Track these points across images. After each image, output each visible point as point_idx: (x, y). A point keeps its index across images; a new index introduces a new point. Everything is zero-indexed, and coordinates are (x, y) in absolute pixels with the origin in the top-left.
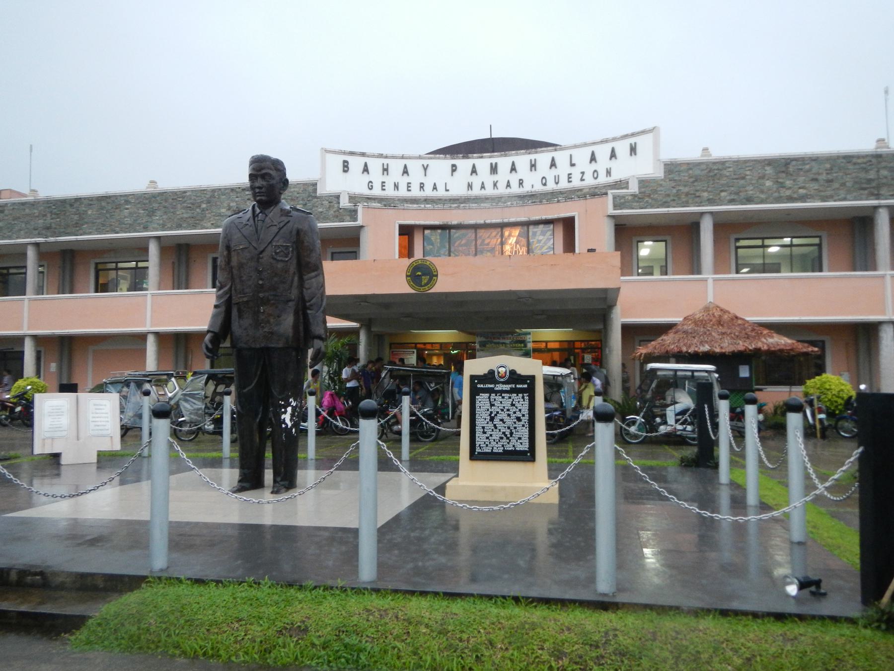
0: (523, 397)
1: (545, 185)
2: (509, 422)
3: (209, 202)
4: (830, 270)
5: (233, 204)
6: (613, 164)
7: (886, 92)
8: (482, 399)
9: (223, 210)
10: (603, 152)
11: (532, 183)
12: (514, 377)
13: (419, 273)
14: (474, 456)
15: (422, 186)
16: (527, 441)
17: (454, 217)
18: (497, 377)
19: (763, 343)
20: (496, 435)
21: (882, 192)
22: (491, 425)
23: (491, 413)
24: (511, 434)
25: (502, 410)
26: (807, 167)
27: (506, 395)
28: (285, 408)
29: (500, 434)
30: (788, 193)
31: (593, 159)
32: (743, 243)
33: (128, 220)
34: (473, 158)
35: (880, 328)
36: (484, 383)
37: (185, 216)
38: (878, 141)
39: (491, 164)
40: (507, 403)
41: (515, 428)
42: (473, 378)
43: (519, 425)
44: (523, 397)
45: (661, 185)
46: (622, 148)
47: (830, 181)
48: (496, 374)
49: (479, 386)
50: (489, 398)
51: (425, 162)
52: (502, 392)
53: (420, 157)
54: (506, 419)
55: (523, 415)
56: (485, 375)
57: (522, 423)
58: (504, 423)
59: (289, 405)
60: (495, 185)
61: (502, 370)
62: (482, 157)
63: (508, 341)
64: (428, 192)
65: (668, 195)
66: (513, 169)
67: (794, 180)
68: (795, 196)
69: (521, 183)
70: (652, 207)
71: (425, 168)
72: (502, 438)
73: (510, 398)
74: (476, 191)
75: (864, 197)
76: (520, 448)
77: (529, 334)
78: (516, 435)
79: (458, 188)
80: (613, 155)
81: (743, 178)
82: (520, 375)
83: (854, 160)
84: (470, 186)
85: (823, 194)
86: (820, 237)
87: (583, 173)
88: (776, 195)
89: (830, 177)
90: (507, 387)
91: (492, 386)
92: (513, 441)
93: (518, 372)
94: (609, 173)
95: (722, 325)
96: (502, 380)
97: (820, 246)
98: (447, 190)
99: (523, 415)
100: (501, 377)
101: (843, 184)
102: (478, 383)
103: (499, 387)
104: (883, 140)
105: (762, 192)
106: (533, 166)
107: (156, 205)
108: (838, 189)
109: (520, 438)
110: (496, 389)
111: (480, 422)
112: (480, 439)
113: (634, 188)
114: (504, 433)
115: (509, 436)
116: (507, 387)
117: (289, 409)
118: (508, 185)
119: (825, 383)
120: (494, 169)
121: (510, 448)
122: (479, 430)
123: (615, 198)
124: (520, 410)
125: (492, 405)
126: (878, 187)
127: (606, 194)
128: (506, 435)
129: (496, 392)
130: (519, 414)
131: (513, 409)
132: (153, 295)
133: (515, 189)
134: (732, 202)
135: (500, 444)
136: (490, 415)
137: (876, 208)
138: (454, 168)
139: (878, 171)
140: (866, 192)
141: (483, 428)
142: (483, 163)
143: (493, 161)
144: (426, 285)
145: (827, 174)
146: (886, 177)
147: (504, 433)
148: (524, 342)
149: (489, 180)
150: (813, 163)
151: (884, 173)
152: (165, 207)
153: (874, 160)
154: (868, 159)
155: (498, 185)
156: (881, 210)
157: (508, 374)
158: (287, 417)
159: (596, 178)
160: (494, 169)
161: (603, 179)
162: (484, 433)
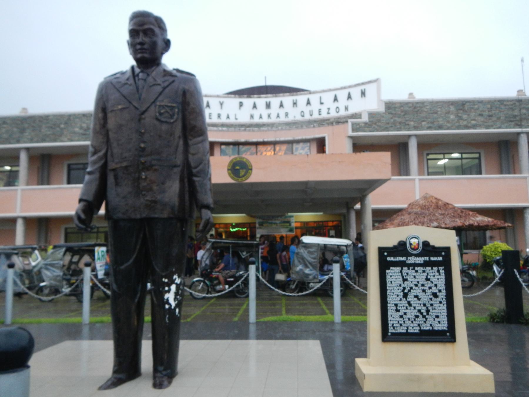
0: (438, 271)
1: (303, 116)
3: (66, 123)
4: (487, 174)
5: (84, 125)
6: (350, 103)
7: (522, 60)
8: (393, 273)
9: (77, 130)
10: (342, 95)
11: (295, 115)
12: (428, 249)
13: (238, 168)
14: (387, 336)
15: (219, 116)
16: (446, 319)
17: (242, 137)
18: (409, 249)
19: (473, 220)
20: (411, 313)
21: (523, 124)
22: (404, 302)
23: (404, 288)
24: (428, 311)
25: (416, 285)
26: (476, 106)
27: (420, 269)
28: (169, 285)
29: (415, 312)
30: (465, 123)
31: (336, 99)
32: (431, 156)
33: (5, 136)
34: (254, 98)
35: (525, 211)
36: (395, 256)
37: (49, 133)
38: (519, 91)
39: (267, 103)
40: (421, 278)
41: (432, 305)
42: (381, 250)
43: (435, 301)
44: (438, 271)
45: (383, 117)
46: (356, 92)
47: (490, 116)
48: (408, 245)
49: (389, 259)
50: (401, 272)
51: (221, 100)
52: (415, 265)
53: (218, 96)
54: (421, 295)
55: (440, 291)
56: (395, 247)
57: (439, 299)
58: (419, 299)
59: (172, 282)
60: (269, 116)
61: (414, 241)
62: (260, 97)
63: (278, 222)
64: (224, 120)
65: (388, 123)
66: (281, 105)
67: (468, 115)
68: (469, 125)
69: (287, 115)
70: (378, 131)
71: (221, 104)
72: (417, 317)
73: (424, 272)
74: (256, 120)
75: (512, 126)
76: (438, 327)
77: (292, 216)
78: (433, 313)
79: (244, 117)
80: (349, 97)
81: (436, 113)
82: (433, 247)
83: (505, 103)
84: (252, 117)
85: (486, 124)
86: (480, 153)
87: (329, 109)
88: (457, 124)
89: (490, 113)
91: (403, 259)
92: (430, 319)
93: (432, 243)
94: (346, 108)
95: (440, 209)
96: (415, 252)
97: (479, 158)
98: (236, 119)
99: (440, 291)
100: (414, 249)
101: (499, 118)
102: (387, 256)
103: (412, 260)
104: (522, 91)
105: (448, 122)
106: (295, 104)
107: (26, 125)
108: (496, 121)
109: (437, 317)
110: (408, 262)
111: (392, 299)
112: (393, 317)
113: (365, 118)
115: (425, 314)
116: (420, 260)
117: (173, 287)
118: (278, 116)
119: (498, 248)
120: (268, 106)
121: (426, 327)
123: (353, 124)
124: (436, 285)
125: (405, 280)
126: (521, 120)
127: (347, 122)
128: (422, 314)
129: (409, 266)
130: (434, 290)
131: (428, 284)
132: (23, 190)
133: (283, 119)
134: (429, 128)
135: (415, 323)
136: (403, 291)
137: (518, 134)
138: (241, 104)
139: (520, 110)
140: (513, 123)
141: (396, 305)
142: (261, 101)
143: (268, 100)
144: (243, 176)
145: (489, 111)
146: (525, 114)
147: (419, 311)
148: (289, 222)
149: (265, 113)
150: (480, 105)
151: (524, 111)
152: (33, 126)
153: (517, 104)
154: (514, 102)
155: (271, 116)
156: (522, 135)
157: (421, 245)
158: (170, 297)
159: (338, 112)
160: (268, 106)
161: (343, 113)
162: (397, 311)
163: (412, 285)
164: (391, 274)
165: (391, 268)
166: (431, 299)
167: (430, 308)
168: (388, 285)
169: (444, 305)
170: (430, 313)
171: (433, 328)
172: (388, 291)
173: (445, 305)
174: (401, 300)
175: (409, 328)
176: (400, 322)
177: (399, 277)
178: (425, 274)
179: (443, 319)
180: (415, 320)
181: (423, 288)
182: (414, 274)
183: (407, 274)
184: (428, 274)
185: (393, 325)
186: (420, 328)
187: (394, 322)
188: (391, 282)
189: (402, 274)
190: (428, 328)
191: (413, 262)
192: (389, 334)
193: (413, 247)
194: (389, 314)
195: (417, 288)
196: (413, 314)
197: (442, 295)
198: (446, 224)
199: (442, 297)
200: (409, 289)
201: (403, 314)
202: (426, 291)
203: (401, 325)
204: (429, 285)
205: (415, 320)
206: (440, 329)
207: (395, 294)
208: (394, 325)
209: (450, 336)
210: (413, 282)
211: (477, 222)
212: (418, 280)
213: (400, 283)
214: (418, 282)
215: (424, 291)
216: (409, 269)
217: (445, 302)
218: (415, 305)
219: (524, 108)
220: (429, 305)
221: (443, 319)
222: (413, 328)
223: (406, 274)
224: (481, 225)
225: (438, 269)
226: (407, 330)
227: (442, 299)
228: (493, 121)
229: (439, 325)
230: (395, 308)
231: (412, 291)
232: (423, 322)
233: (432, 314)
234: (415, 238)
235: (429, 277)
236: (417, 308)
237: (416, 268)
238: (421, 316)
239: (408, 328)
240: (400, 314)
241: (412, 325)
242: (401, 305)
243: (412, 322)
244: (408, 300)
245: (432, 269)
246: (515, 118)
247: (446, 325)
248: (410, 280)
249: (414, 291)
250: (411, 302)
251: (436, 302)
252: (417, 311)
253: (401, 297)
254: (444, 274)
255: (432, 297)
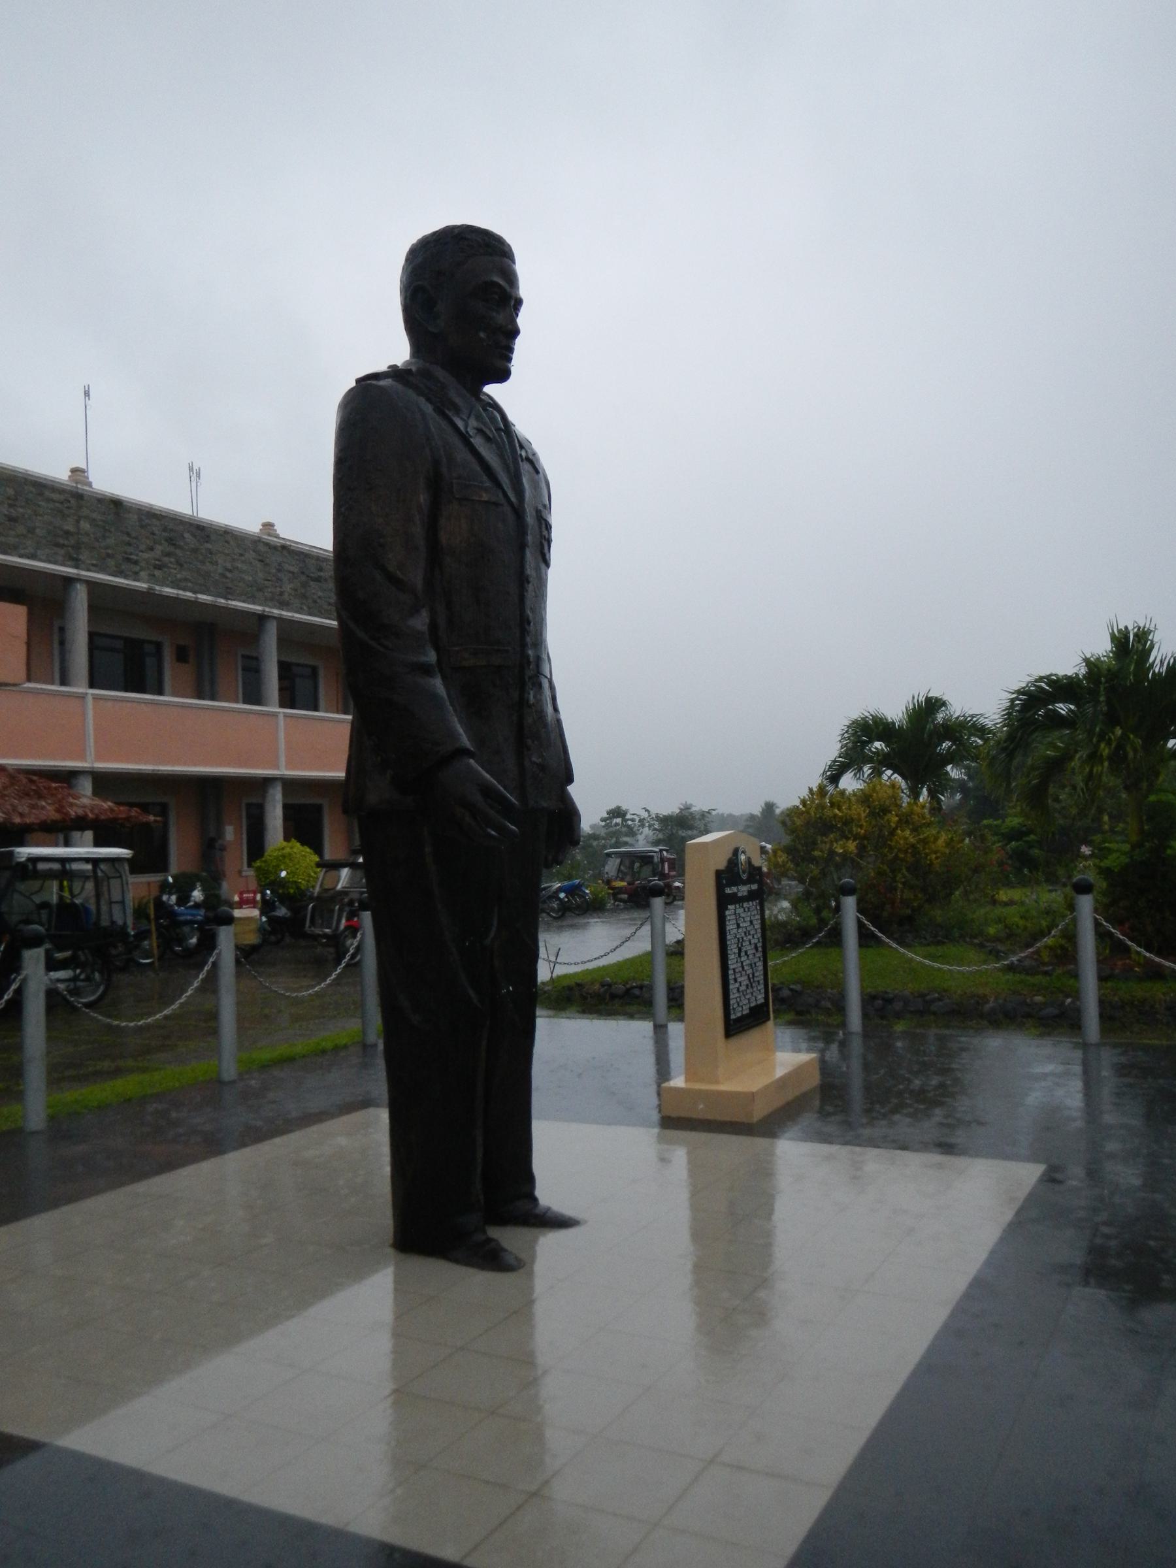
7: (87, 394)
38: (75, 471)
75: (60, 558)
89: (13, 513)
101: (31, 531)
104: (83, 471)
108: (24, 536)
126: (77, 547)
137: (69, 581)
139: (78, 521)
140: (62, 552)
145: (10, 506)
146: (87, 534)
151: (85, 526)
153: (73, 501)
198: (21, 815)
211: (92, 811)
219: (86, 517)
224: (103, 817)
228: (18, 536)
246: (67, 539)
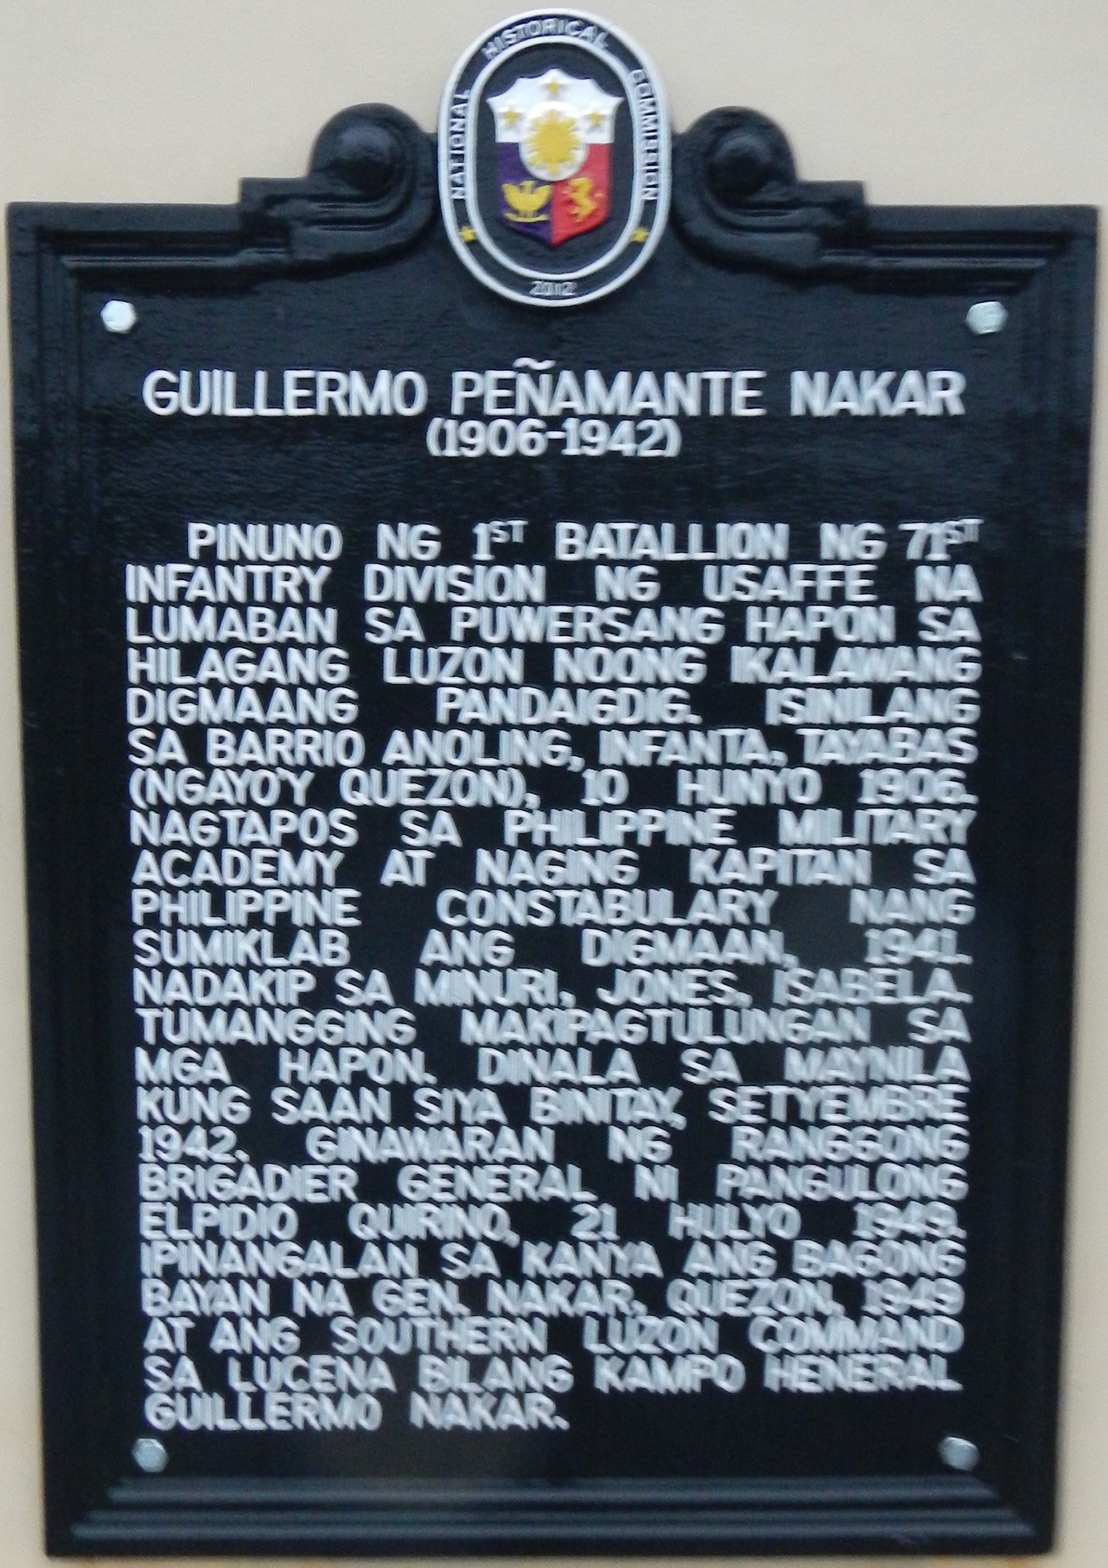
0: (893, 581)
2: (663, 970)
8: (229, 619)
16: (943, 1257)
20: (463, 1175)
22: (371, 1028)
24: (700, 1149)
25: (555, 788)
27: (620, 549)
40: (635, 676)
41: (761, 1062)
43: (818, 1014)
44: (893, 581)
48: (457, 184)
49: (165, 394)
50: (344, 592)
52: (549, 491)
54: (618, 920)
55: (894, 866)
56: (264, 209)
57: (866, 986)
58: (586, 985)
61: (554, 119)
72: (545, 1221)
73: (679, 585)
76: (822, 1355)
78: (771, 1164)
90: (633, 411)
91: (383, 394)
92: (726, 1260)
93: (817, 162)
96: (551, 289)
99: (894, 866)
102: (138, 351)
103: (509, 412)
109: (830, 1221)
110: (454, 440)
111: (202, 979)
112: (208, 1238)
114: (580, 1144)
116: (633, 411)
121: (671, 1360)
122: (178, 1096)
124: (841, 787)
125: (389, 709)
128: (611, 1180)
129: (456, 499)
130: (816, 849)
131: (732, 771)
135: (519, 1313)
136: (360, 867)
141: (253, 1066)
147: (580, 1144)
157: (652, 184)
162: (271, 1142)
163: (486, 789)
164: (186, 626)
165: (198, 535)
166: (756, 981)
167: (736, 1108)
168: (146, 784)
169: (931, 1056)
170: (727, 1177)
171: (754, 1362)
172: (146, 869)
173: (953, 1064)
174: (323, 994)
175: (429, 1369)
176: (303, 1297)
177: (309, 665)
178: (692, 624)
179: (912, 1257)
180: (510, 1264)
181: (646, 822)
182: (529, 626)
183: (435, 617)
184: (733, 616)
185: (203, 1327)
186: (583, 1366)
187: (225, 1299)
188: (194, 738)
189: (352, 631)
190: (686, 1377)
191: (525, 440)
192: (150, 1454)
193: (525, 202)
194: (156, 1184)
195: (566, 825)
196: (484, 1183)
197: (924, 925)
199: (926, 947)
200: (446, 831)
201: (344, 1182)
202: (700, 866)
203: (316, 1334)
204: (746, 789)
205: (510, 1264)
206: (850, 1377)
207: (238, 908)
208: (223, 1339)
209: (978, 1472)
210: (513, 745)
212: (586, 710)
213: (329, 749)
214: (585, 740)
215: (662, 866)
216: (457, 549)
217: (955, 1027)
218: (516, 1068)
220: (726, 1067)
221: (912, 1257)
222: (478, 1367)
223: (410, 626)
225: (897, 542)
226: (395, 1404)
227: (921, 971)
229: (843, 1332)
230: (231, 1106)
231: (486, 862)
232: (618, 1296)
233: (751, 1182)
234: (577, 63)
235: (746, 666)
236: (549, 1107)
237: (570, 540)
238: (597, 1217)
239: (405, 1368)
240: (302, 1183)
241: (466, 1335)
242: (324, 1068)
243: (473, 1293)
244: (425, 990)
245: (805, 547)
247: (945, 1335)
248: (470, 706)
249: (524, 868)
250: (471, 1029)
251: (825, 1027)
252: (542, 1145)
253: (334, 950)
254: (964, 625)
255: (767, 946)
